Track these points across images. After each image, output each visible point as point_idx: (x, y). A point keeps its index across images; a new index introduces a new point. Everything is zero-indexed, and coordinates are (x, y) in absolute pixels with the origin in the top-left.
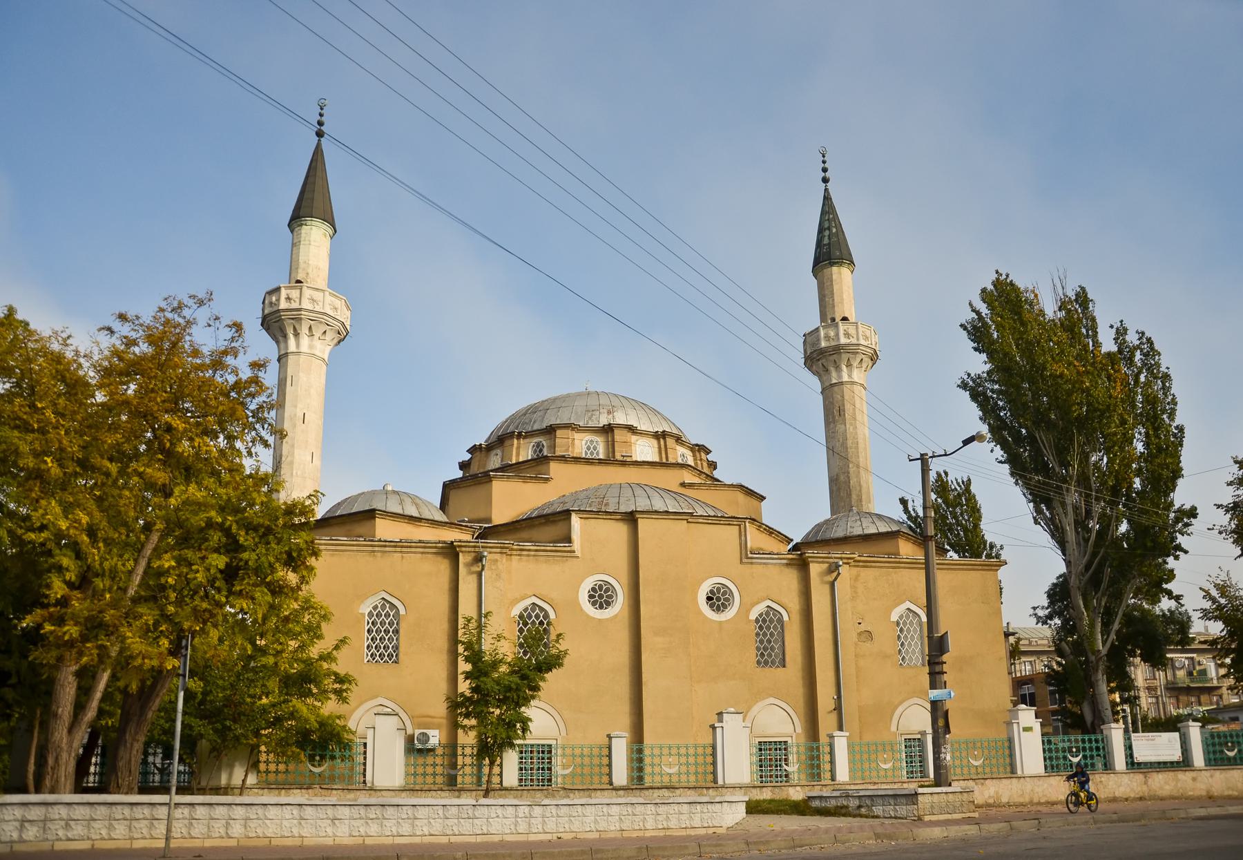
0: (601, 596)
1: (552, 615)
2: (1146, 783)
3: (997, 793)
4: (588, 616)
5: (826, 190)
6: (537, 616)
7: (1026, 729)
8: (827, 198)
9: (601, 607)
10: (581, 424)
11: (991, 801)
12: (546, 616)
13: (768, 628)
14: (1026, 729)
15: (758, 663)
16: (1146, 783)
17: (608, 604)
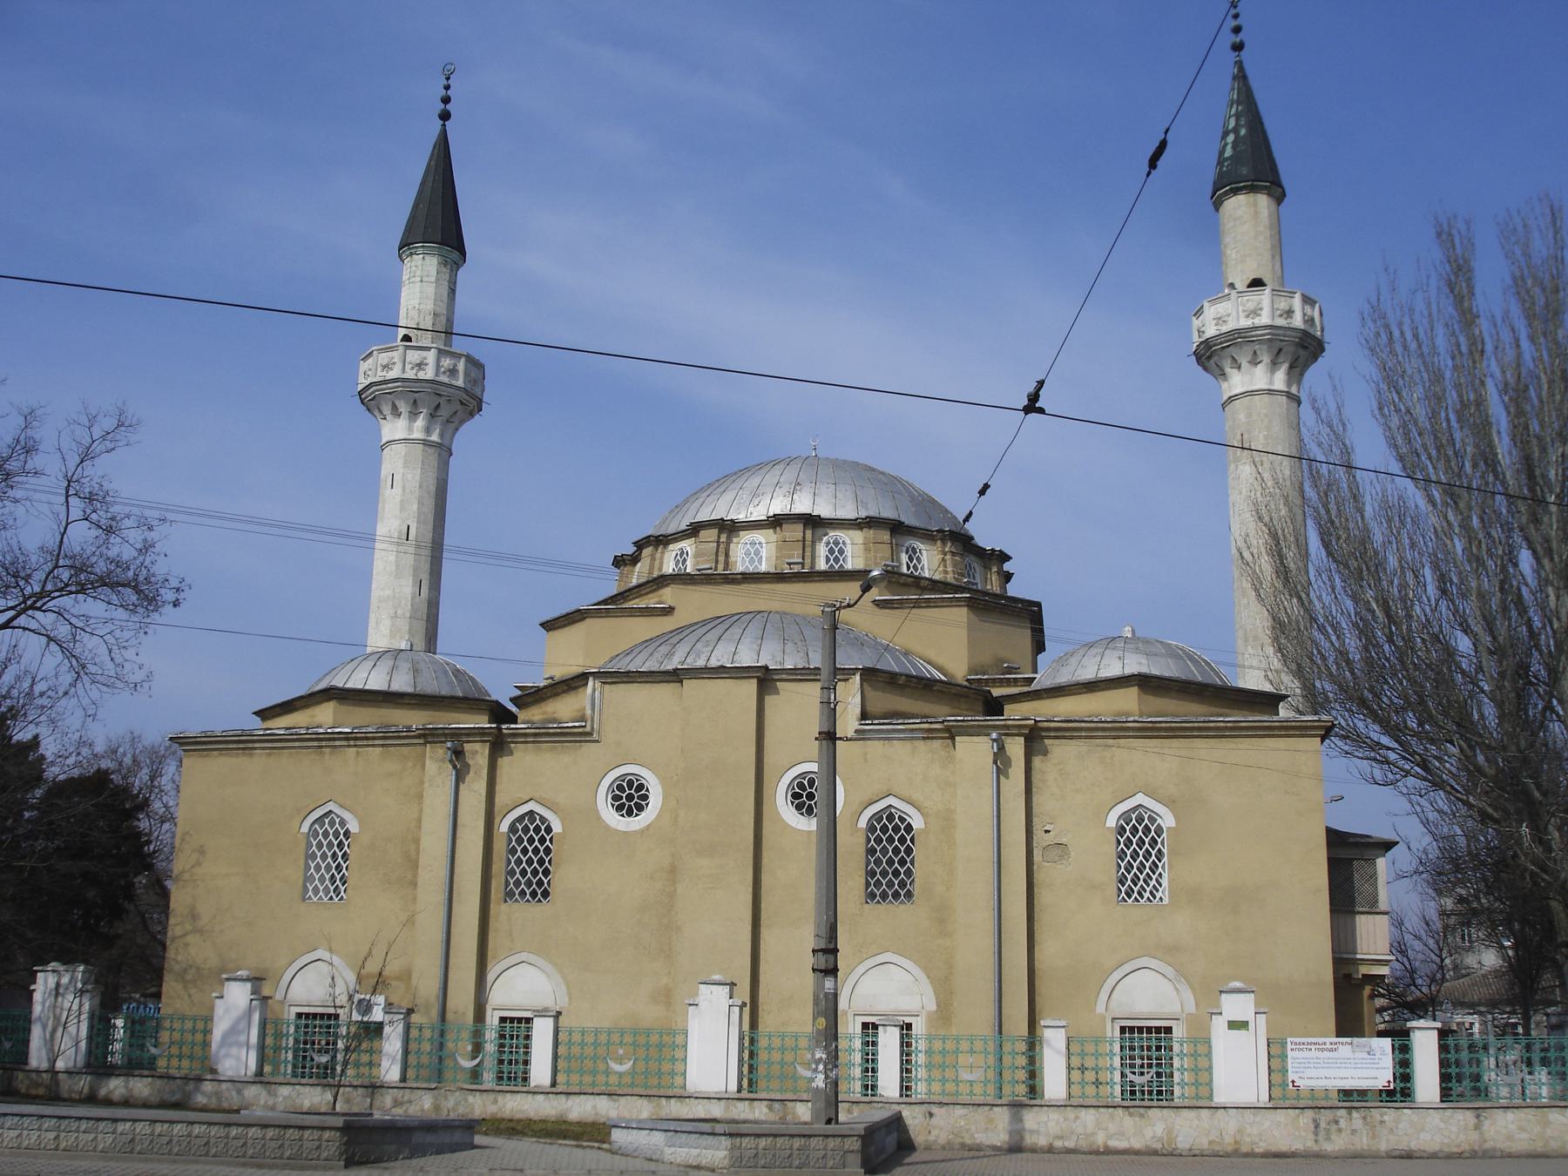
0: (630, 798)
1: (557, 827)
2: (1477, 1127)
3: (1169, 1131)
4: (607, 827)
5: (1240, 64)
6: (537, 829)
7: (1233, 1025)
8: (1241, 77)
9: (630, 813)
10: (741, 517)
11: (1158, 1146)
12: (549, 830)
13: (891, 840)
14: (1233, 1025)
15: (872, 896)
16: (1477, 1127)
17: (640, 808)
